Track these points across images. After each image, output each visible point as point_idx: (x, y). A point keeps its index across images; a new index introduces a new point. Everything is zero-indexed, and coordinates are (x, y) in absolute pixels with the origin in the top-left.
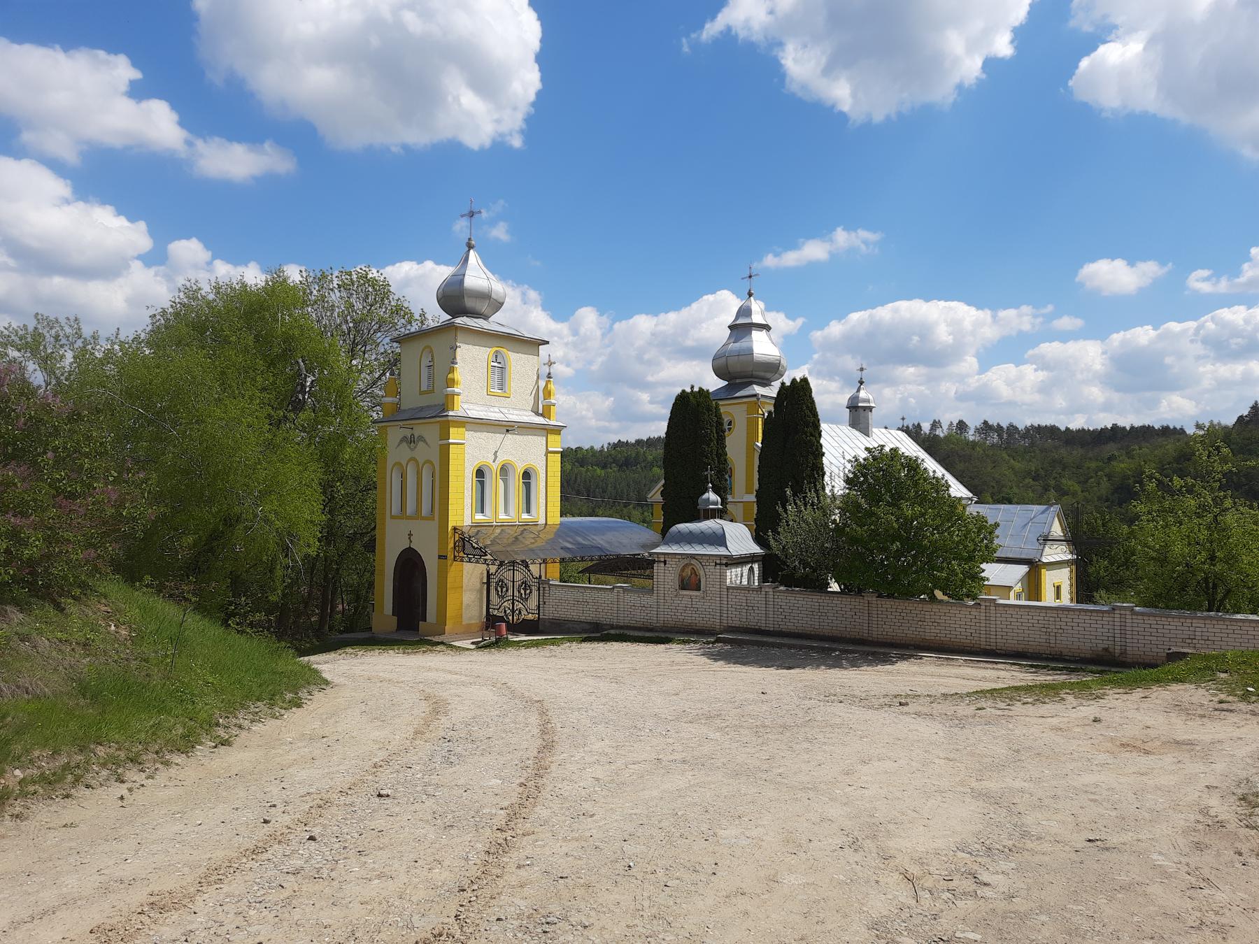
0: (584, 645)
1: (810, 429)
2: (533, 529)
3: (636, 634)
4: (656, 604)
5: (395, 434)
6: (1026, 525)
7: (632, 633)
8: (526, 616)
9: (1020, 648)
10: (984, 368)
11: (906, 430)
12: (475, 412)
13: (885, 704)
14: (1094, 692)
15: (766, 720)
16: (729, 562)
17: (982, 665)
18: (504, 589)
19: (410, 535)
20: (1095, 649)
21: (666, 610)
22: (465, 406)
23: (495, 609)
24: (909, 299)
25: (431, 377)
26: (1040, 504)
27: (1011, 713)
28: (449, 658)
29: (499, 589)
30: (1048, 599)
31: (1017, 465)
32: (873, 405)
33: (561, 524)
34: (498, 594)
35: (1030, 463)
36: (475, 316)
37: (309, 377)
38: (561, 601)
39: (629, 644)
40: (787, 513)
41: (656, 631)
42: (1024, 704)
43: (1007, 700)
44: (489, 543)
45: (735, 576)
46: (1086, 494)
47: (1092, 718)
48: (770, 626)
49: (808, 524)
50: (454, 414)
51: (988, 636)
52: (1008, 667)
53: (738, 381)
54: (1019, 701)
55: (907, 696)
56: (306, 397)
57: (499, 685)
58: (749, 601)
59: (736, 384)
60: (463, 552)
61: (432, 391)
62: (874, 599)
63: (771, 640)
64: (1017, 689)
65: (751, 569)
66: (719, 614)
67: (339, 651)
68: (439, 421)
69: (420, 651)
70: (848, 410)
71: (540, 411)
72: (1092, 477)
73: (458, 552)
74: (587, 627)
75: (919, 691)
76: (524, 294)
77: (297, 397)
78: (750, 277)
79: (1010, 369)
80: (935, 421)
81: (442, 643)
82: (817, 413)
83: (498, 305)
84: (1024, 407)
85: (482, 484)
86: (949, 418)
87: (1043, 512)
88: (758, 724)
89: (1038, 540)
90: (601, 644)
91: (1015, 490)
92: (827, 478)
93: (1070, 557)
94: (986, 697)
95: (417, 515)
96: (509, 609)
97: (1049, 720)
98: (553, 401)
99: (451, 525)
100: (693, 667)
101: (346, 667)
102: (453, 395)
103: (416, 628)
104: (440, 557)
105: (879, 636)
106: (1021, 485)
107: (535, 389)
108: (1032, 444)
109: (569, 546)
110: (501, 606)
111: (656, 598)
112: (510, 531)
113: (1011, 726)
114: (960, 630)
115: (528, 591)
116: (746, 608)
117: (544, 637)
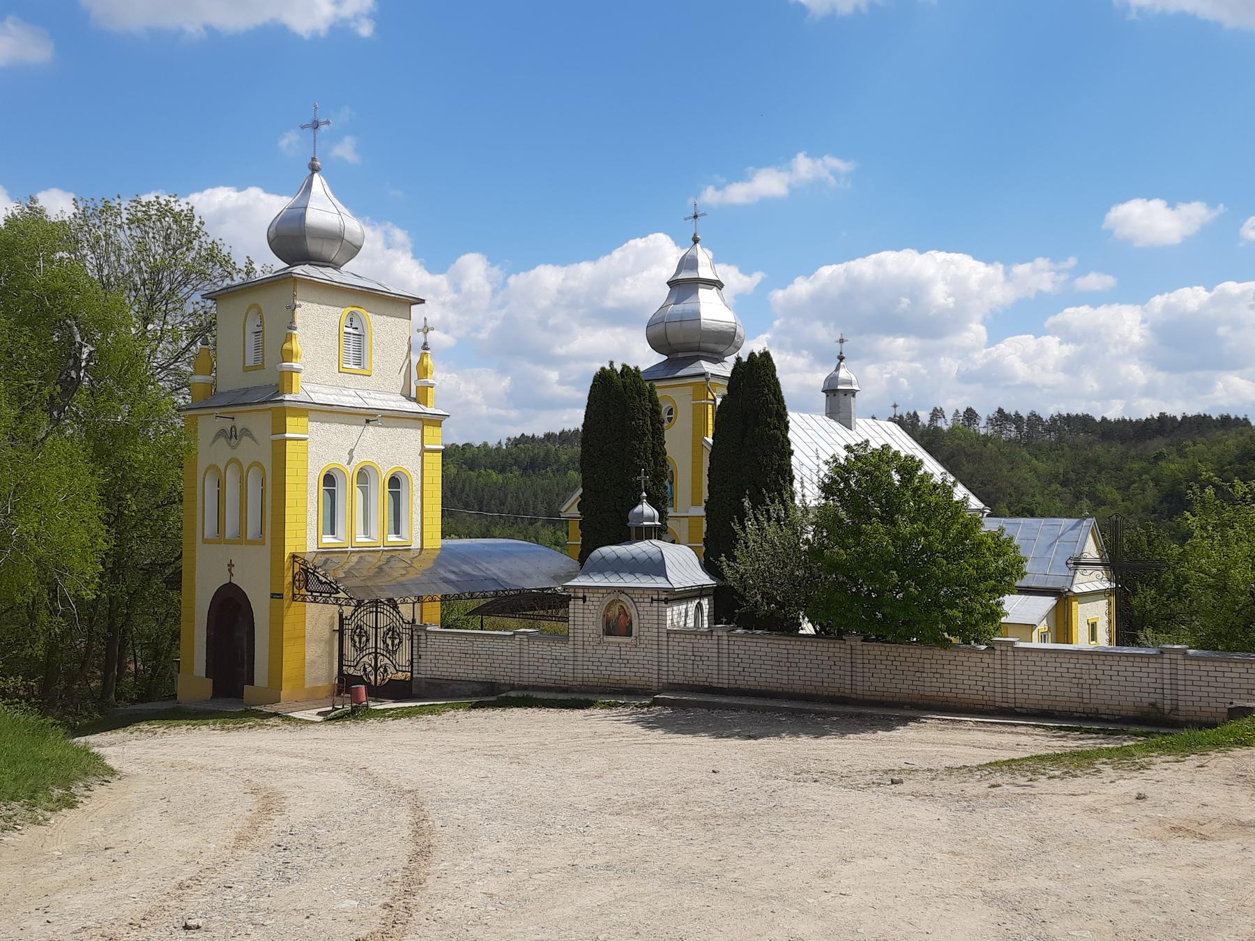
0: (473, 712)
1: (773, 420)
2: (403, 555)
3: (545, 696)
4: (572, 655)
5: (209, 425)
6: (1052, 544)
7: (539, 695)
8: (392, 674)
9: (1045, 705)
10: (994, 338)
11: (899, 421)
12: (322, 396)
13: (873, 783)
14: (1137, 761)
15: (717, 808)
16: (670, 597)
17: (997, 728)
18: (364, 639)
19: (231, 565)
20: (1140, 704)
21: (585, 663)
22: (308, 388)
23: (350, 666)
24: (898, 248)
25: (259, 347)
26: (1070, 517)
27: (1033, 791)
29: (357, 639)
30: (1081, 640)
31: (1041, 466)
32: (857, 388)
33: (443, 548)
34: (355, 646)
35: (1057, 464)
36: (321, 264)
38: (442, 654)
39: (536, 710)
40: (745, 532)
41: (573, 692)
42: (1050, 778)
43: (1028, 774)
44: (343, 575)
45: (678, 616)
46: (1128, 503)
48: (724, 681)
49: (773, 546)
50: (292, 399)
51: (1005, 690)
52: (1030, 730)
53: (680, 355)
54: (1044, 774)
55: (901, 771)
57: (356, 771)
58: (696, 649)
59: (678, 359)
60: (306, 588)
61: (262, 367)
62: (859, 643)
63: (725, 700)
64: (1041, 758)
65: (699, 606)
66: (656, 668)
67: (131, 728)
68: (270, 409)
69: (245, 726)
70: (825, 394)
71: (413, 395)
72: (1134, 482)
73: (299, 589)
74: (478, 688)
75: (918, 764)
76: (386, 233)
78: (696, 217)
79: (1027, 341)
80: (935, 409)
81: (276, 714)
82: (782, 397)
83: (353, 250)
84: (1046, 391)
85: (332, 494)
86: (952, 405)
87: (1073, 528)
88: (706, 813)
89: (1067, 564)
90: (498, 711)
91: (1038, 498)
92: (796, 485)
93: (1107, 585)
94: (1002, 771)
95: (241, 538)
96: (371, 666)
97: (1082, 798)
98: (430, 381)
99: (289, 550)
100: (621, 739)
101: (140, 751)
102: (292, 371)
103: (237, 694)
104: (273, 596)
105: (865, 693)
106: (1046, 492)
107: (406, 364)
108: (1060, 439)
109: (452, 577)
110: (360, 662)
111: (572, 647)
112: (374, 560)
113: (1033, 807)
114: (969, 682)
115: (397, 641)
116: (693, 658)
117: (419, 704)
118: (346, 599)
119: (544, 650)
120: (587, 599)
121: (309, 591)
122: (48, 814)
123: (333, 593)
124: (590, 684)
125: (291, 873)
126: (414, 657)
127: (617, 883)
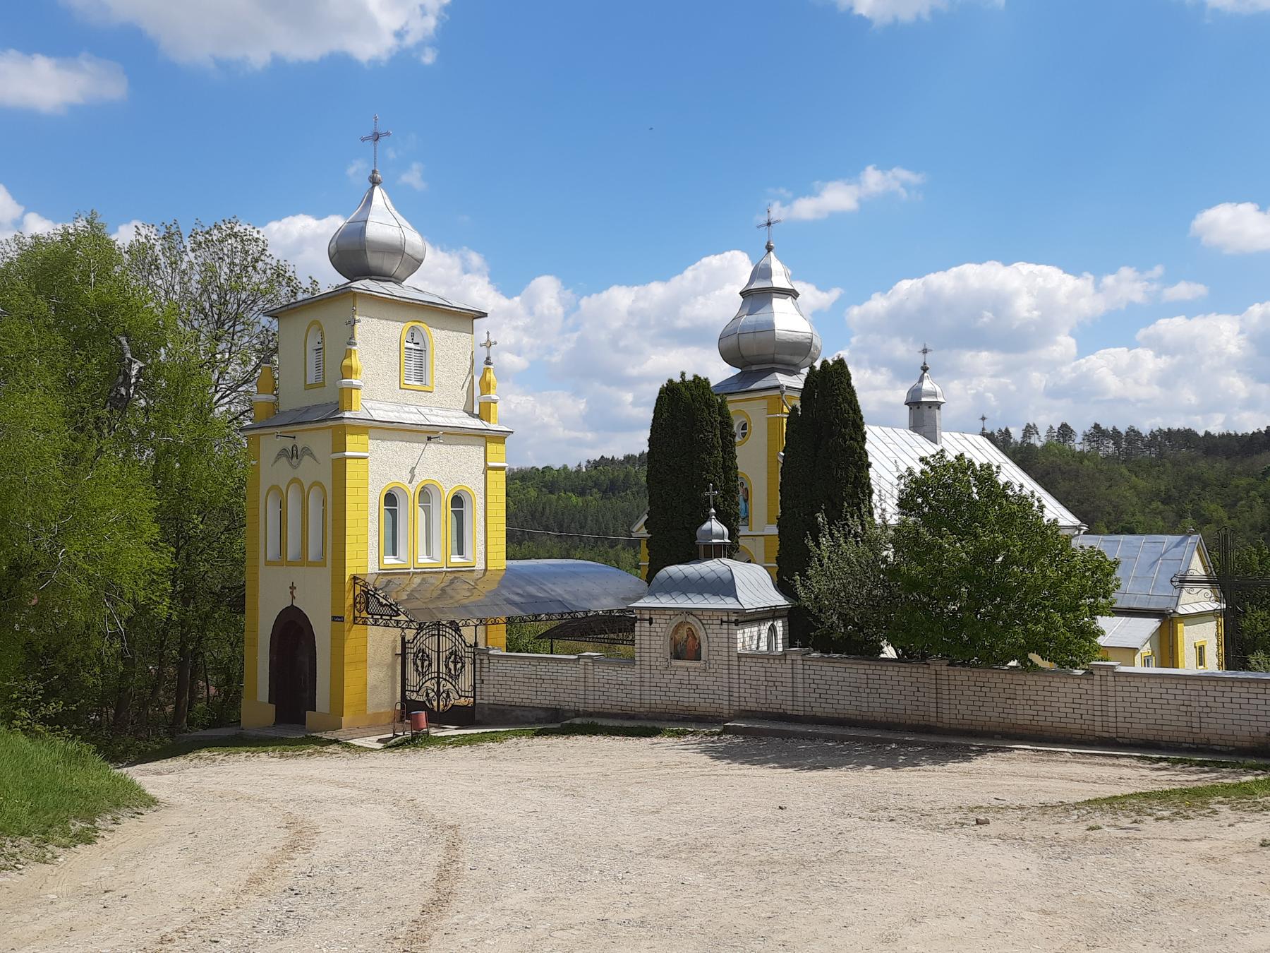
0: (536, 740)
2: (466, 577)
4: (639, 680)
5: (271, 445)
6: (1155, 562)
7: (604, 722)
8: (455, 700)
9: (1150, 735)
12: (382, 412)
16: (740, 619)
17: (1097, 760)
18: (426, 663)
19: (293, 588)
21: (652, 688)
22: (368, 405)
23: (413, 691)
25: (320, 365)
26: (1173, 534)
28: (342, 764)
29: (419, 663)
31: (1142, 484)
32: (940, 399)
33: (508, 569)
34: (417, 670)
35: (1158, 481)
36: (382, 278)
37: (135, 362)
38: (505, 679)
39: (601, 738)
40: (819, 549)
41: (640, 719)
42: (1157, 819)
43: (1132, 814)
44: (406, 597)
45: (750, 638)
46: (1235, 521)
47: (1259, 841)
48: (799, 708)
49: (849, 563)
50: (352, 417)
51: (1105, 719)
52: (1134, 762)
53: (754, 368)
56: (131, 391)
58: (768, 674)
59: (752, 371)
60: (367, 611)
61: (322, 385)
62: (944, 668)
63: (800, 728)
64: (1147, 796)
65: (772, 629)
66: (727, 693)
67: (191, 756)
68: (330, 427)
69: (304, 754)
70: (907, 407)
71: (476, 411)
72: (1242, 499)
74: (542, 714)
75: (1010, 800)
77: (118, 392)
81: (336, 742)
83: (415, 264)
85: (394, 513)
87: (1178, 545)
90: (561, 740)
91: (1139, 517)
94: (1102, 810)
95: (302, 560)
96: (433, 691)
98: (494, 397)
99: (349, 572)
102: (351, 388)
103: (301, 721)
104: (334, 619)
105: (952, 721)
106: (1147, 510)
107: (468, 380)
108: (1161, 456)
109: (516, 598)
110: (423, 687)
111: (639, 671)
112: (434, 581)
114: (1067, 710)
115: (459, 665)
116: (765, 683)
117: (481, 731)
118: (406, 621)
119: (610, 674)
120: (654, 621)
121: (370, 614)
122: (60, 851)
123: (394, 616)
124: (658, 710)
125: (291, 925)
126: (476, 681)
127: (648, 944)
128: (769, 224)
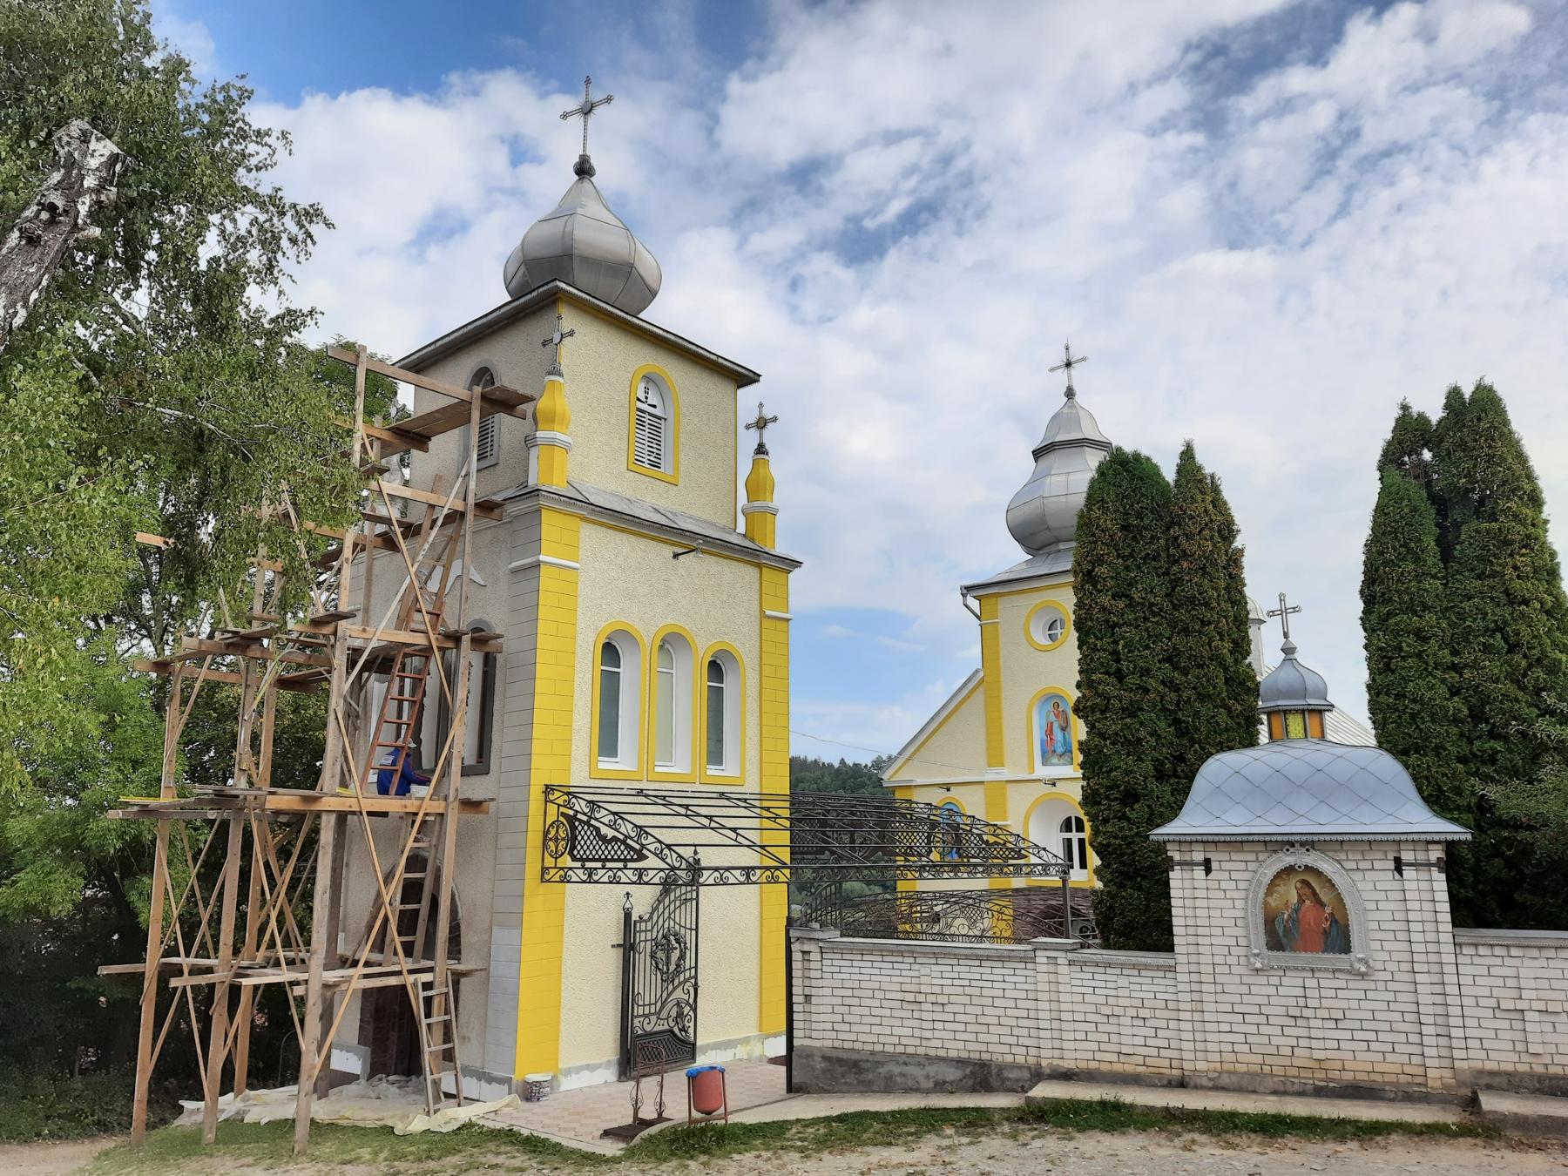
60: (571, 854)
73: (556, 856)
74: (952, 1074)
118: (662, 870)
119: (1109, 985)
120: (1214, 865)
121: (578, 860)
123: (632, 860)
124: (1242, 1068)
126: (795, 999)
128: (1068, 365)
